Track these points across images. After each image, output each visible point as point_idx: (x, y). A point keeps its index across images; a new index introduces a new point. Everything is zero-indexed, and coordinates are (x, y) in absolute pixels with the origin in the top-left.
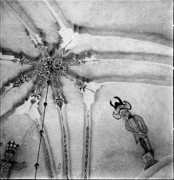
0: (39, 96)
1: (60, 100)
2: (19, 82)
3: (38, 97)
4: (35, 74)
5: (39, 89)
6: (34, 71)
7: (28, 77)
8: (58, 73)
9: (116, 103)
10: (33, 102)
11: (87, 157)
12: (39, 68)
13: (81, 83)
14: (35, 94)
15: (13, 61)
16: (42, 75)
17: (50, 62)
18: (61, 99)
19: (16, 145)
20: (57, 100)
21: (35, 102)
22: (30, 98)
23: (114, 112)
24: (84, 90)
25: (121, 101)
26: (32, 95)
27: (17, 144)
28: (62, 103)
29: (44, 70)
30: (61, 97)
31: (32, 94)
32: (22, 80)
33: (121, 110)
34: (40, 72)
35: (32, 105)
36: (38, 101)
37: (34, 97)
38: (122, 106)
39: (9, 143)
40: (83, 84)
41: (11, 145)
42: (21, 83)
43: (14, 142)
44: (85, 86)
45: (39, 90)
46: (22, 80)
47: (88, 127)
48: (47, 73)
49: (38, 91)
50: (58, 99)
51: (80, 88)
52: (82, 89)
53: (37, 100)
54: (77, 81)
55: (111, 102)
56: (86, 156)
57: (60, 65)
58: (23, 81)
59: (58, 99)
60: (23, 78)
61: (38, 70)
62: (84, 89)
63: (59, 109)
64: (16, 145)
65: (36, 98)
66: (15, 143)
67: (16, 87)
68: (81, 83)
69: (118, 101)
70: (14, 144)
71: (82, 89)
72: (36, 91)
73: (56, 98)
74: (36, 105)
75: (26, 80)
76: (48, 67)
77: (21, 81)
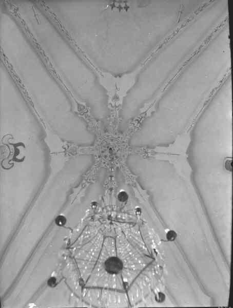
0: (111, 108)
3: (112, 106)
4: (126, 135)
9: (17, 152)
10: (116, 98)
12: (124, 145)
15: (156, 153)
19: (115, 6)
20: (86, 111)
22: (120, 102)
23: (13, 138)
25: (16, 161)
27: (114, 8)
30: (84, 117)
33: (9, 152)
36: (110, 101)
38: (11, 158)
39: (127, 8)
41: (123, 5)
42: (139, 119)
43: (120, 10)
44: (66, 154)
45: (113, 116)
47: (33, 106)
48: (112, 140)
49: (115, 115)
50: (87, 112)
51: (68, 147)
52: (66, 147)
57: (103, 161)
58: (137, 122)
59: (87, 112)
61: (124, 142)
62: (64, 150)
63: (79, 102)
64: (115, 6)
66: (118, 10)
69: (19, 157)
70: (120, 8)
71: (66, 147)
74: (111, 96)
77: (139, 122)
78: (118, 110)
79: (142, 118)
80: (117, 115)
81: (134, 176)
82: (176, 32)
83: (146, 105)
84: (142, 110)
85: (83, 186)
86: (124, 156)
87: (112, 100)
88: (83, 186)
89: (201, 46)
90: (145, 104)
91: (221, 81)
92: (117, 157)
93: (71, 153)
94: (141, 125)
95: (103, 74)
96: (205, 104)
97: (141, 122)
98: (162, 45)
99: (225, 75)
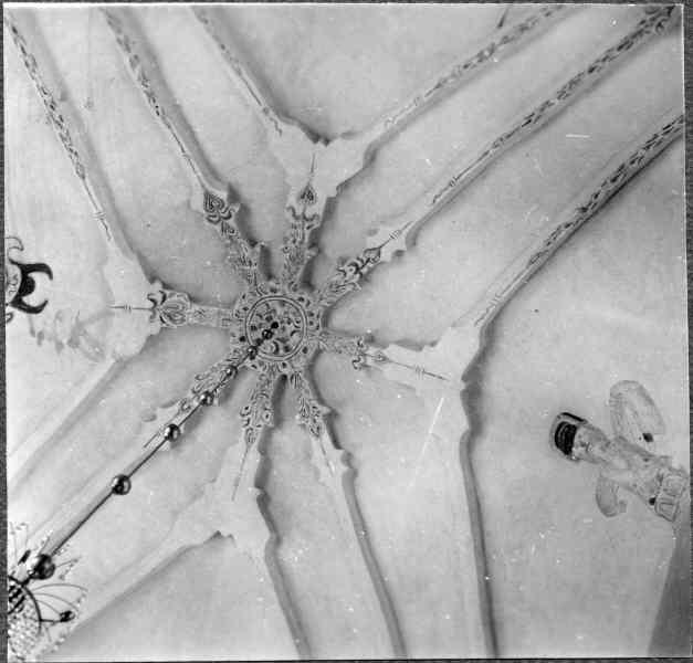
1: (215, 219)
3: (294, 215)
5: (297, 243)
6: (324, 307)
7: (338, 287)
9: (27, 287)
10: (308, 195)
11: (27, 65)
12: (311, 323)
13: (169, 323)
14: (307, 225)
15: (385, 359)
17: (281, 352)
20: (225, 215)
21: (303, 197)
22: (318, 208)
24: (152, 300)
25: (20, 308)
26: (315, 222)
28: (207, 211)
29: (294, 313)
31: (316, 225)
32: (355, 273)
34: (304, 304)
35: (307, 180)
37: (309, 214)
40: (164, 322)
42: (359, 263)
45: (294, 242)
46: (355, 273)
47: (83, 177)
48: (283, 303)
49: (299, 239)
50: (226, 218)
51: (164, 298)
53: (296, 206)
54: (183, 320)
55: (51, 276)
56: (35, 63)
58: (354, 269)
59: (226, 218)
60: (354, 281)
61: (312, 315)
62: (151, 304)
65: (299, 212)
67: (374, 249)
68: (171, 319)
69: (31, 300)
71: (159, 297)
72: (307, 237)
73: (231, 222)
75: (345, 274)
76: (284, 329)
78: (308, 228)
79: (368, 261)
80: (306, 240)
81: (320, 408)
82: (487, 53)
83: (385, 232)
84: (373, 242)
85: (186, 407)
86: (305, 350)
87: (298, 200)
88: (186, 407)
89: (548, 104)
90: (382, 228)
91: (584, 210)
92: (287, 349)
93: (169, 316)
94: (364, 279)
95: (282, 126)
96: (531, 262)
97: (364, 270)
98: (445, 81)
99: (596, 196)
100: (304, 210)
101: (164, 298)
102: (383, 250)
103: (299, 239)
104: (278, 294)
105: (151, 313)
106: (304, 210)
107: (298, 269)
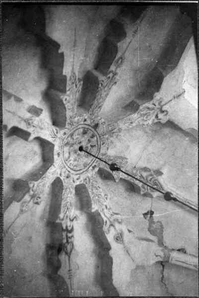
2: (67, 236)
3: (117, 220)
5: (104, 207)
8: (99, 143)
14: (108, 222)
16: (82, 179)
18: (147, 177)
22: (110, 237)
32: (67, 227)
34: (75, 179)
42: (70, 235)
46: (67, 227)
49: (105, 210)
58: (69, 228)
60: (63, 222)
62: (164, 108)
65: (117, 225)
71: (161, 116)
78: (106, 222)
86: (59, 154)
100: (115, 229)
101: (157, 116)
102: (67, 257)
103: (105, 210)
104: (91, 168)
105: (163, 103)
106: (115, 229)
107: (93, 193)
